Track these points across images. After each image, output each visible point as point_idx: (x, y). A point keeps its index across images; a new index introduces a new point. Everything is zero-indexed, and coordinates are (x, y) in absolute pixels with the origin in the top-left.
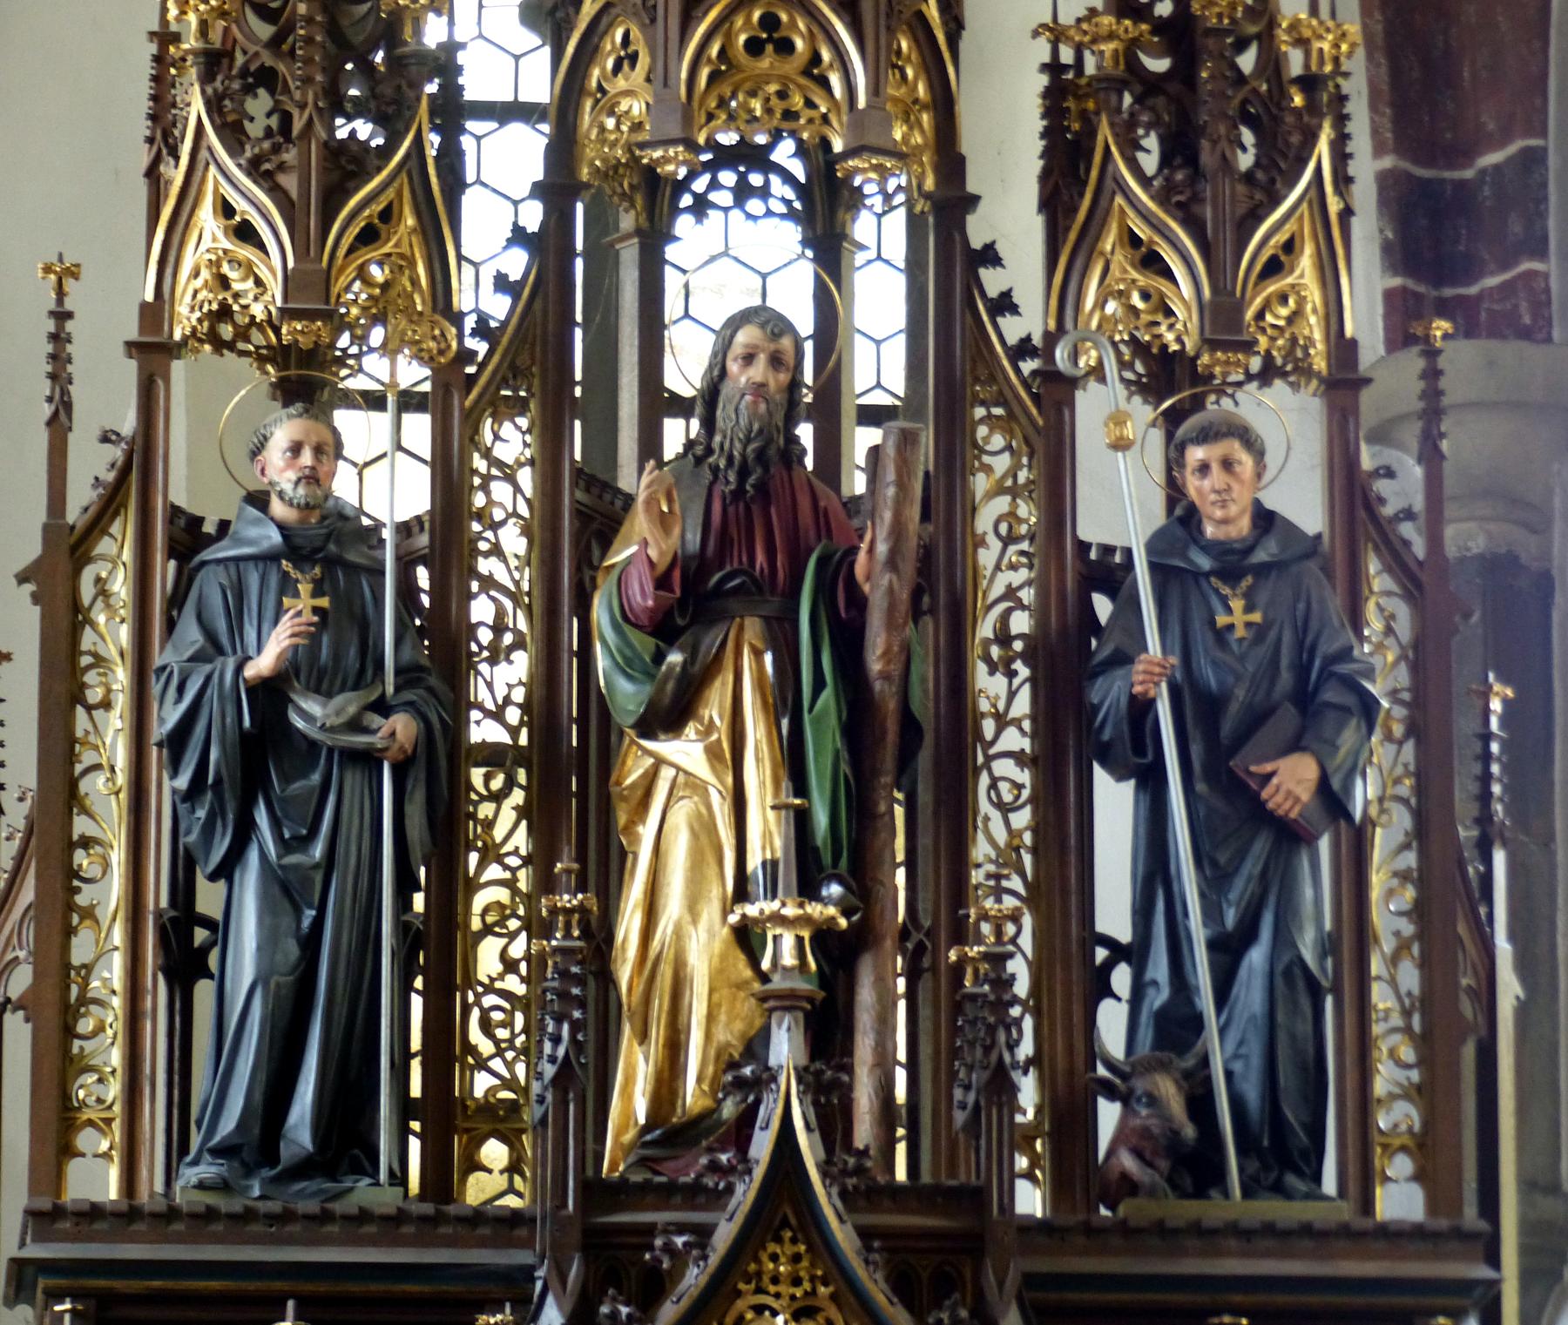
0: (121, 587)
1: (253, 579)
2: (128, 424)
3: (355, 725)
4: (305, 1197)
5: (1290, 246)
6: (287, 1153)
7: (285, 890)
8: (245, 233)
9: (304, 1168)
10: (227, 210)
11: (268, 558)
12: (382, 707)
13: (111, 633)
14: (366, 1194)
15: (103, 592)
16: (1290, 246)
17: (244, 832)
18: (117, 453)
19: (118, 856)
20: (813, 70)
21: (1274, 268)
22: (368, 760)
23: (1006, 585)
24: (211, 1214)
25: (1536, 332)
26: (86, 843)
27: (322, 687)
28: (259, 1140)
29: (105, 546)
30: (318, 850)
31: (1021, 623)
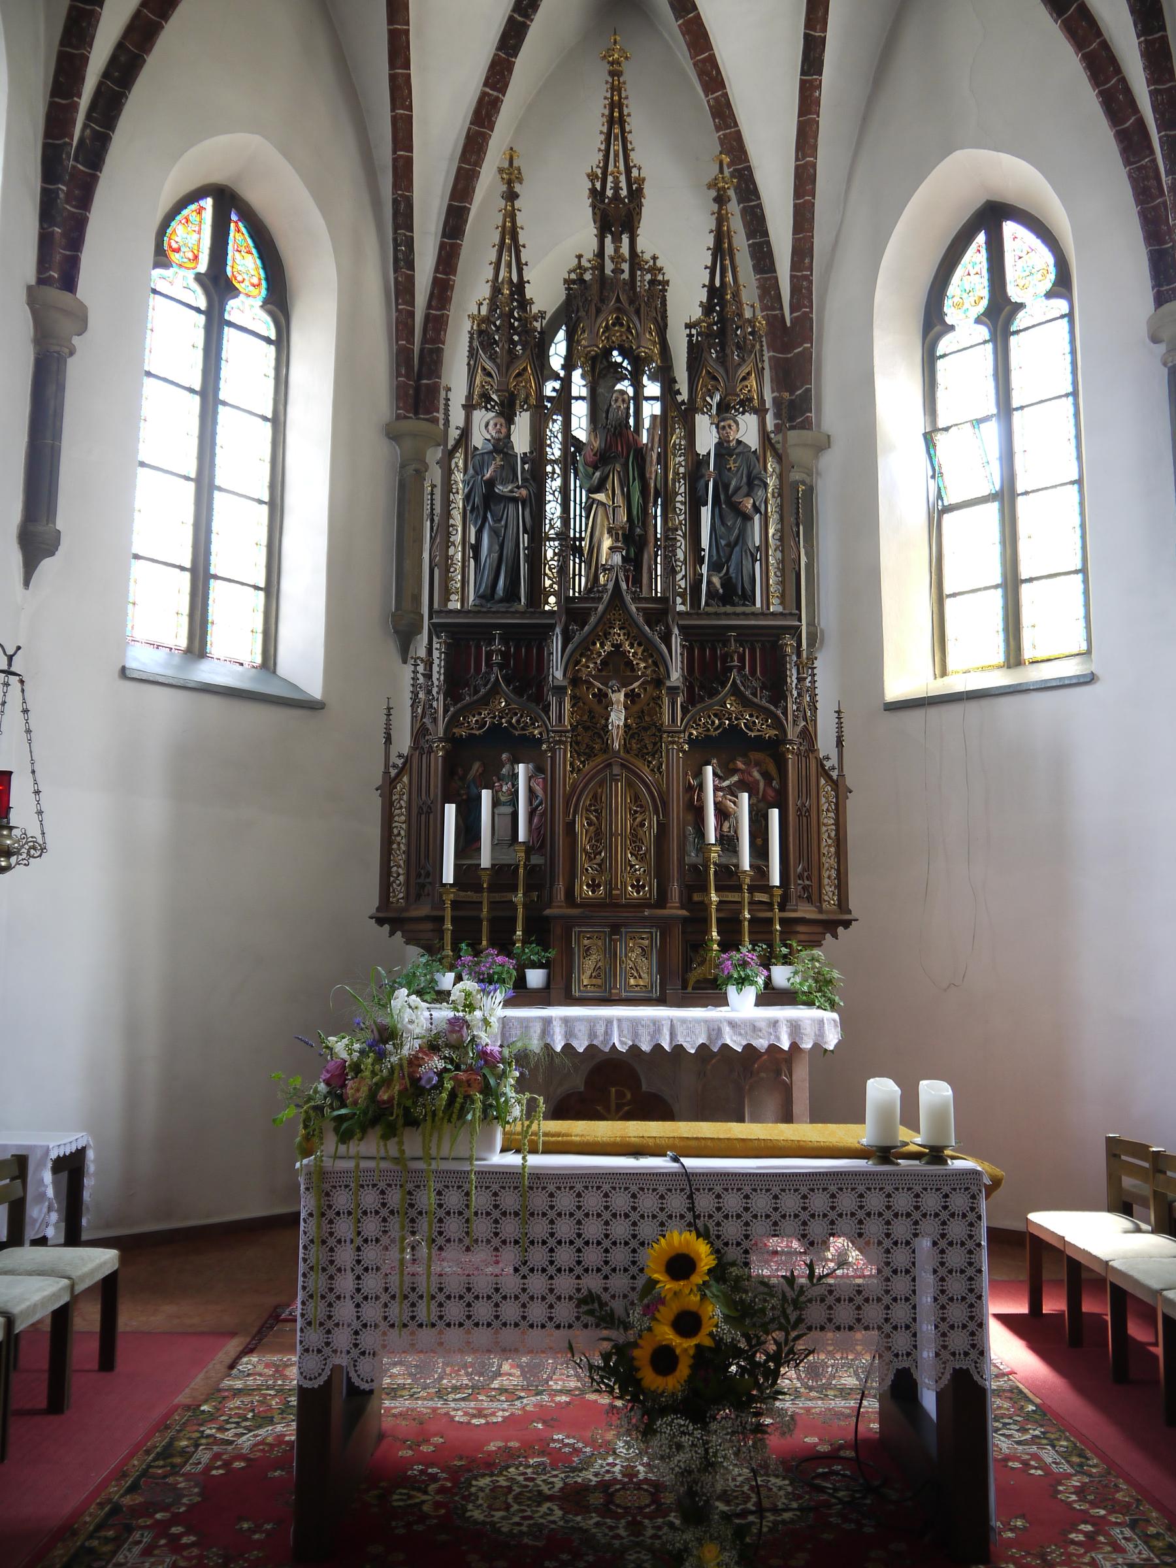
0: (461, 464)
1: (486, 457)
2: (462, 425)
3: (511, 491)
4: (502, 607)
5: (749, 374)
6: (496, 597)
7: (495, 532)
8: (489, 375)
9: (501, 601)
10: (484, 369)
11: (490, 453)
12: (518, 487)
13: (458, 476)
14: (516, 607)
15: (457, 466)
16: (749, 374)
17: (485, 519)
18: (458, 432)
19: (460, 529)
20: (629, 329)
21: (744, 379)
22: (515, 500)
23: (678, 461)
24: (479, 612)
25: (810, 428)
26: (453, 526)
27: (504, 482)
28: (487, 596)
29: (458, 455)
30: (503, 523)
31: (682, 470)
